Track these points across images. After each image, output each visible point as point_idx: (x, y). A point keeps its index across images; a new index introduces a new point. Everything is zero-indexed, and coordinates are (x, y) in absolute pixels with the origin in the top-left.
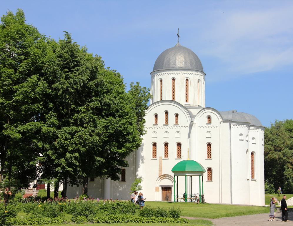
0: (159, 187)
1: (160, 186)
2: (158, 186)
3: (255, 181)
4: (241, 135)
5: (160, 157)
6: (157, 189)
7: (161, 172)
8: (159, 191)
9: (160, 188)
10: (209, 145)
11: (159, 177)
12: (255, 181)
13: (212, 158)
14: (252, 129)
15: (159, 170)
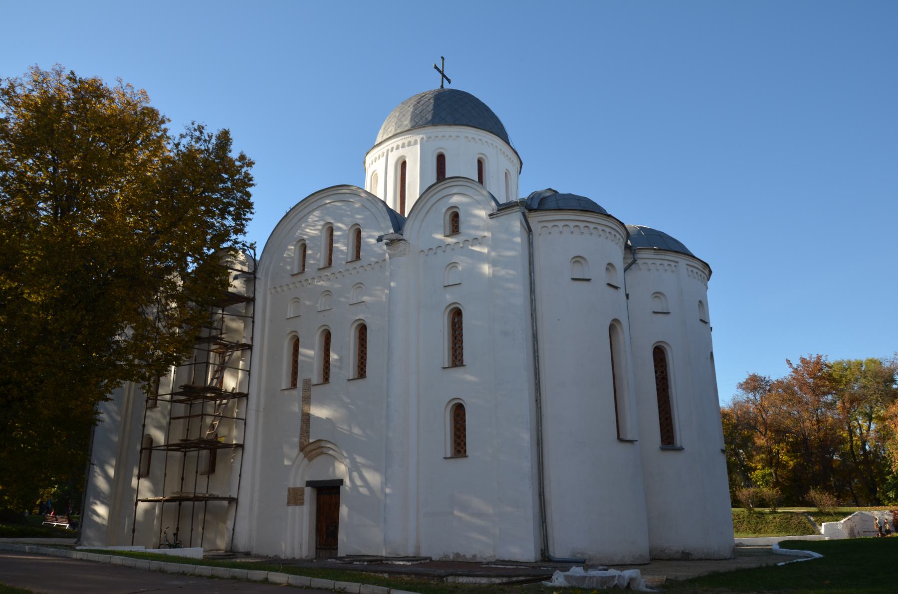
0: (302, 490)
1: (309, 484)
2: (299, 483)
3: (681, 449)
4: (578, 260)
5: (308, 384)
6: (295, 498)
7: (308, 432)
8: (302, 504)
9: (308, 491)
10: (457, 314)
11: (302, 450)
12: (681, 449)
13: (464, 364)
14: (649, 262)
15: (302, 429)
